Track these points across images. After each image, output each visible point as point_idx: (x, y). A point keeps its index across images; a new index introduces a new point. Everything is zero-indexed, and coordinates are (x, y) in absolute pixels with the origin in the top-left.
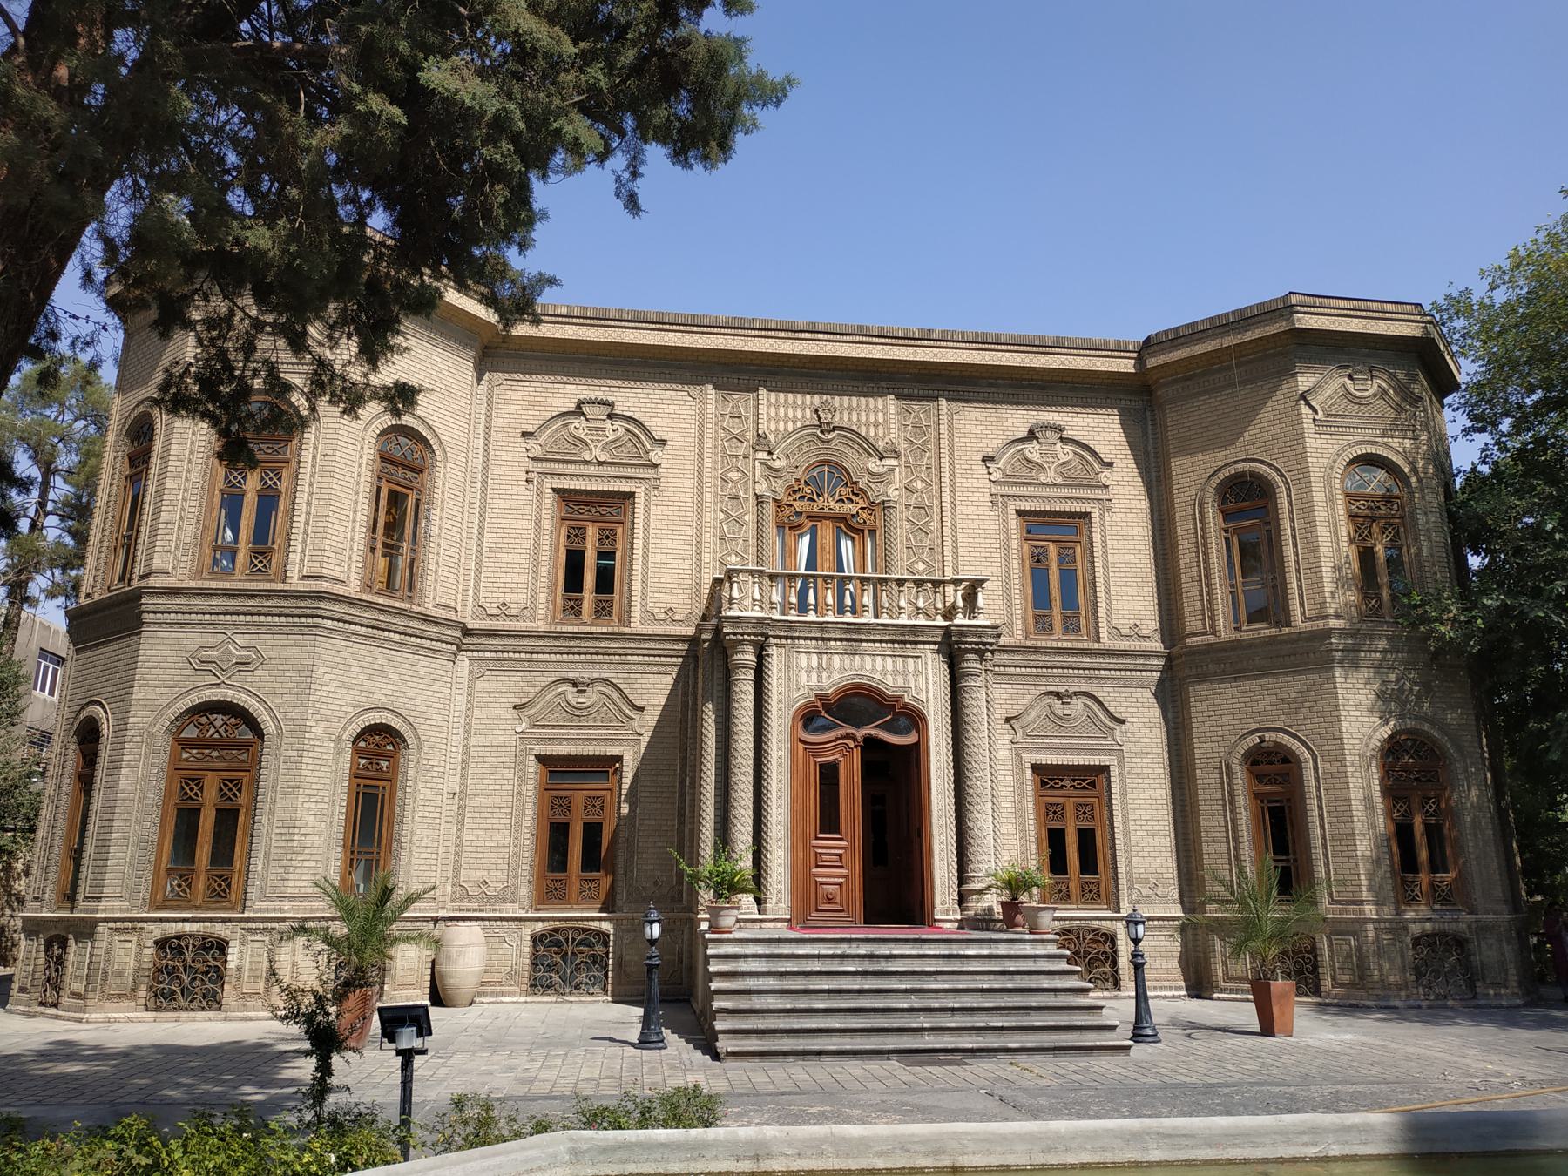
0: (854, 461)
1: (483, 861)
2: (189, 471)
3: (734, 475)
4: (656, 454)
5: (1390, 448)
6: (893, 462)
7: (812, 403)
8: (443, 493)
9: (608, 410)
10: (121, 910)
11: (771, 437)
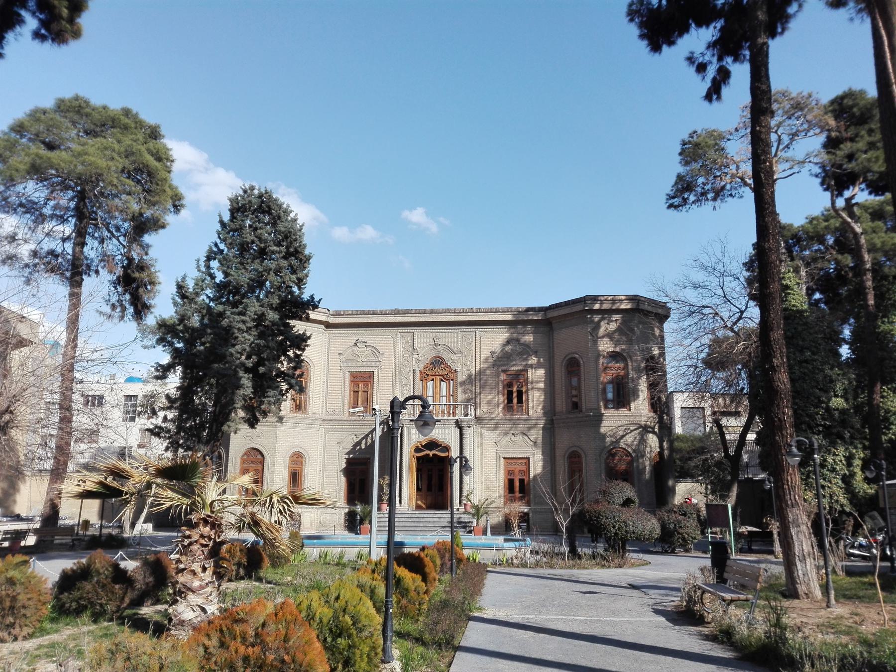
4: (381, 358)
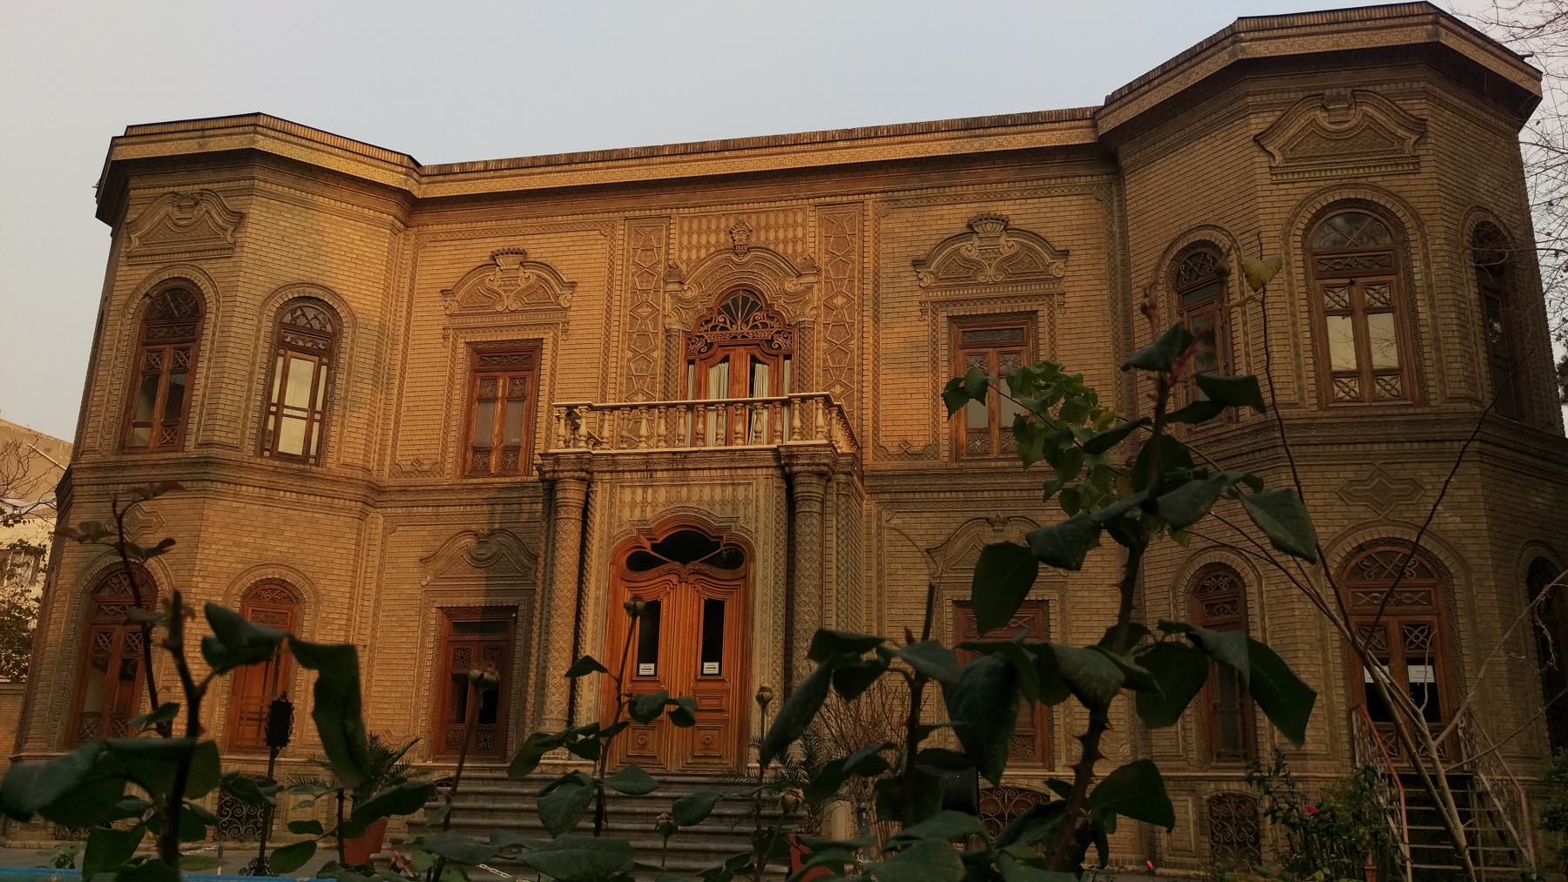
0: (767, 285)
1: (388, 711)
2: (116, 358)
3: (645, 311)
4: (565, 297)
5: (1378, 189)
6: (812, 279)
7: (727, 226)
8: (351, 357)
9: (520, 258)
10: (41, 750)
11: (684, 268)
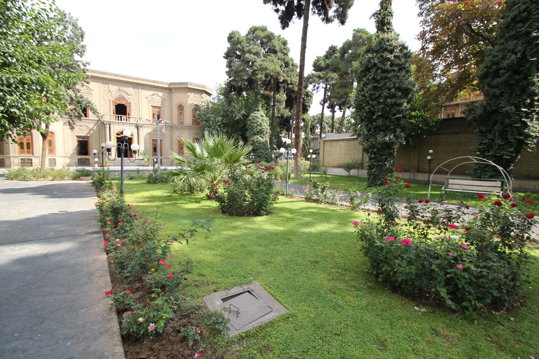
4: (92, 92)
